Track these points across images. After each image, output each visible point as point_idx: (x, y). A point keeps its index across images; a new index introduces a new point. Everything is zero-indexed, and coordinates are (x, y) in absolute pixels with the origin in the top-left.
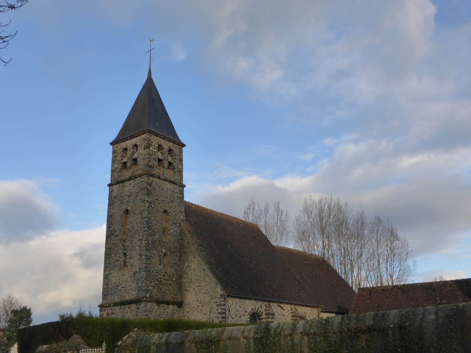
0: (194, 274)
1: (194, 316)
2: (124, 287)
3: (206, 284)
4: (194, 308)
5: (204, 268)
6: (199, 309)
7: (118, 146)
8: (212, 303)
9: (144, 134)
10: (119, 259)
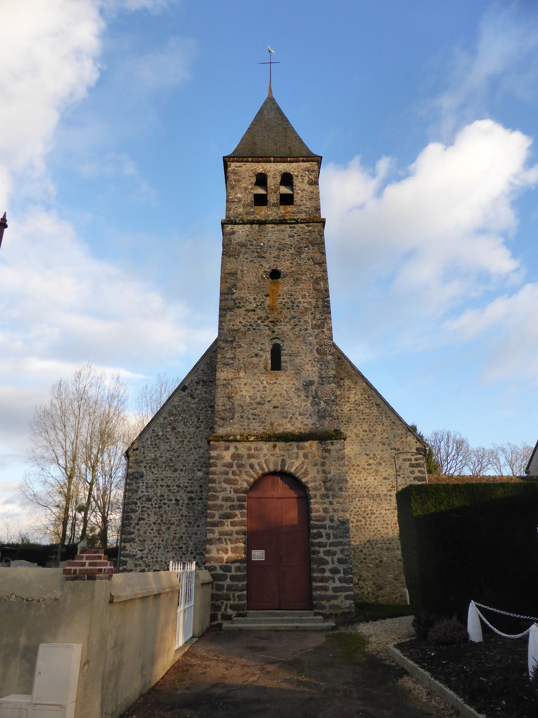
0: (357, 410)
1: (360, 480)
2: (278, 407)
3: (385, 428)
4: (358, 466)
5: (377, 403)
6: (372, 468)
7: (242, 165)
8: (399, 462)
9: (308, 161)
10: (261, 353)
